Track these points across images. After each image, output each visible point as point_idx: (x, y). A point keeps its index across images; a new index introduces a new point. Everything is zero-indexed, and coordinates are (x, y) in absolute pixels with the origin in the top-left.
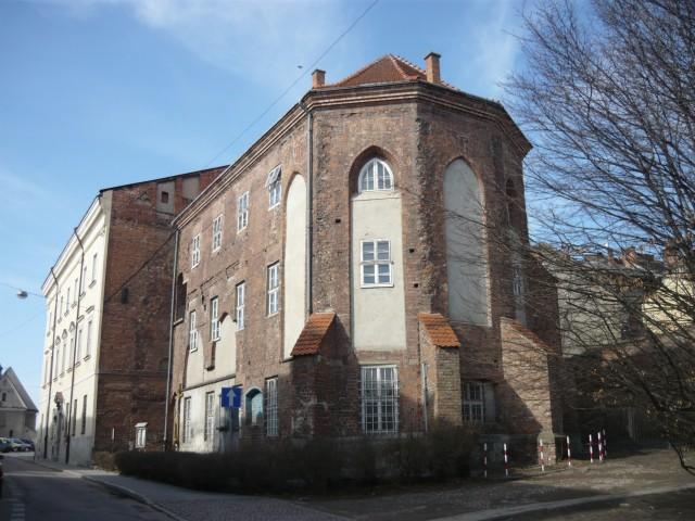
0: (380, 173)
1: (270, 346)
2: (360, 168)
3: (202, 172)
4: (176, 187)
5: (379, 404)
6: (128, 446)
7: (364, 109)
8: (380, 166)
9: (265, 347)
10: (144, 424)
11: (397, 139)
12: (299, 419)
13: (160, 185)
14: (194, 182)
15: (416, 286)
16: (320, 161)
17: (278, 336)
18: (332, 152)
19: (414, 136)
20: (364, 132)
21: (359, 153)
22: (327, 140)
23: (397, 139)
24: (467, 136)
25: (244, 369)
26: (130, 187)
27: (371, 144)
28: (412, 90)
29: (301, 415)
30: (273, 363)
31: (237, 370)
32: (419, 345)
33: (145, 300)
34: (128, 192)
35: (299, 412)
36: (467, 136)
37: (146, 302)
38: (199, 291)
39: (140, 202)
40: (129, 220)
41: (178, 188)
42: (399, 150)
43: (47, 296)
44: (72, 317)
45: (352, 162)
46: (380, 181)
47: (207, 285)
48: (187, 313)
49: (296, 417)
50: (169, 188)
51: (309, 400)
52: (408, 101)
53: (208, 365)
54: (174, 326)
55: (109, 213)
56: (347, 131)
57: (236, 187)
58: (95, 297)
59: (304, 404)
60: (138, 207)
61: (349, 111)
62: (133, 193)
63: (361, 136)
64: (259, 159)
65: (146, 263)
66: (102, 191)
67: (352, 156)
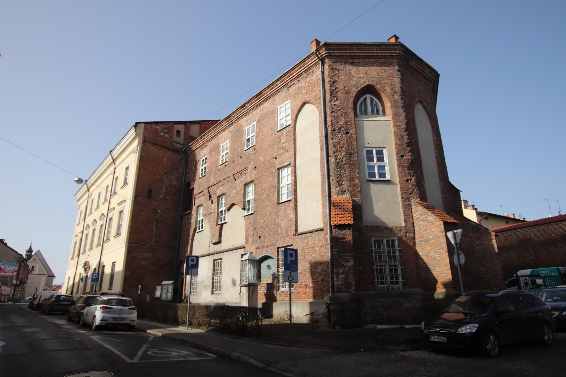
0: (372, 105)
1: (283, 224)
2: (358, 100)
3: (202, 121)
4: (185, 128)
5: (387, 266)
6: (146, 299)
7: (361, 60)
8: (372, 100)
9: (278, 225)
10: (171, 282)
11: (386, 81)
12: (341, 276)
13: (175, 125)
14: (197, 127)
15: (407, 181)
16: (331, 92)
17: (292, 216)
18: (340, 86)
19: (397, 81)
20: (362, 75)
21: (359, 88)
22: (335, 78)
23: (386, 81)
24: (422, 88)
25: (254, 242)
26: (157, 123)
27: (367, 83)
28: (396, 50)
29: (342, 273)
30: (287, 236)
31: (247, 242)
32: (413, 223)
33: (163, 198)
34: (154, 126)
35: (341, 271)
36: (422, 88)
37: (164, 199)
38: (207, 191)
39: (162, 134)
40: (154, 144)
41: (187, 129)
42: (388, 89)
43: (78, 200)
44: (104, 209)
45: (355, 94)
46: (372, 111)
47: (213, 187)
48: (194, 208)
49: (338, 274)
50: (181, 128)
51: (349, 261)
52: (392, 57)
53: (216, 239)
54: (182, 217)
55: (142, 137)
56: (350, 75)
57: (242, 121)
58: (128, 193)
59: (345, 264)
60: (161, 136)
61: (351, 61)
62: (158, 127)
63: (360, 77)
64: (266, 100)
65: (165, 174)
66: (137, 123)
67: (354, 91)
